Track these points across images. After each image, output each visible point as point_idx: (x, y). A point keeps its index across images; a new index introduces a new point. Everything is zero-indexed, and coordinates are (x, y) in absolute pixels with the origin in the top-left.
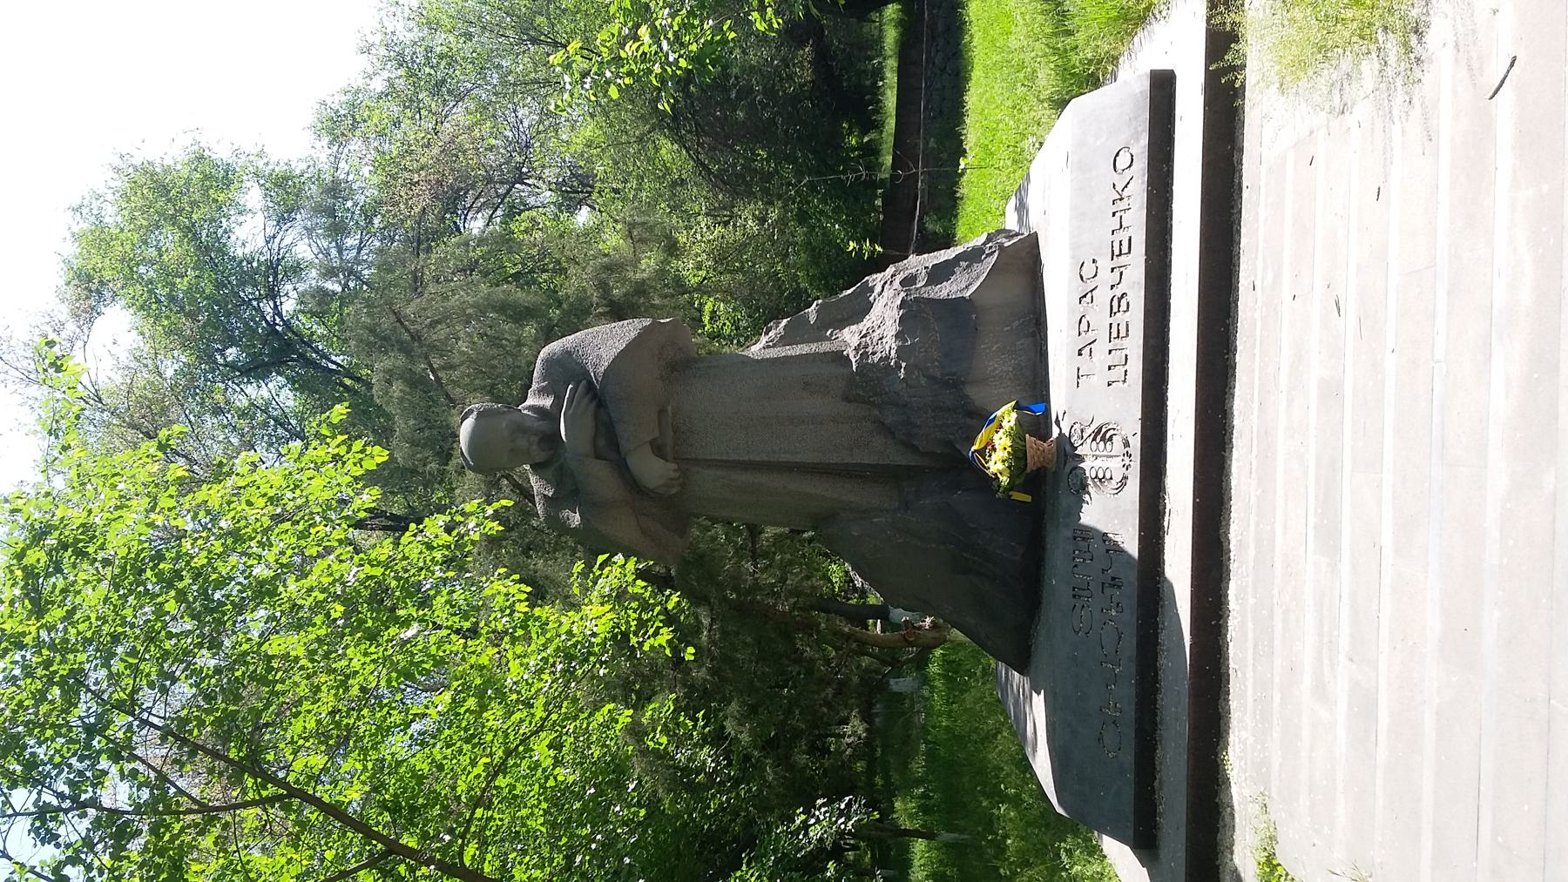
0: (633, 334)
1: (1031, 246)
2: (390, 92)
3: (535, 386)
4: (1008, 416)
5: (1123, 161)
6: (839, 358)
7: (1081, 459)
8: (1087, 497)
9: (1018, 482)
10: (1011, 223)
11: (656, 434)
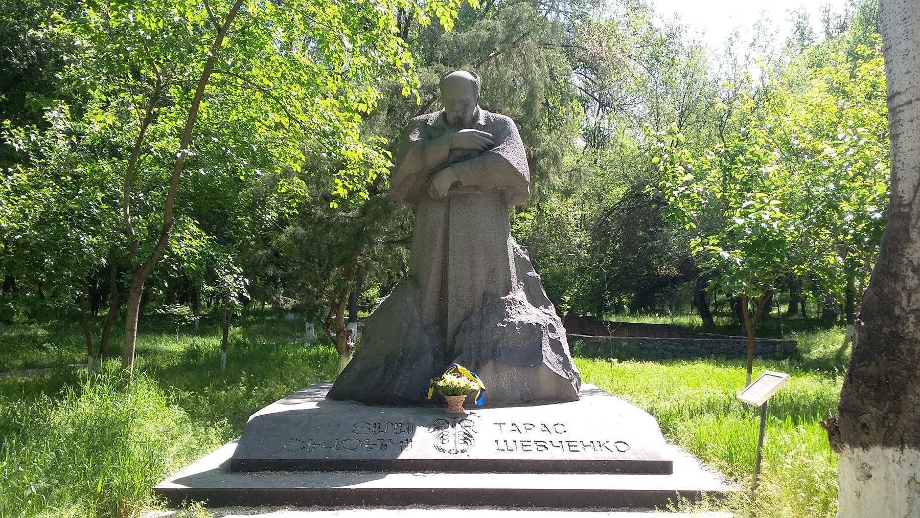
0: (521, 171)
1: (573, 398)
2: (652, 30)
3: (490, 114)
4: (477, 385)
5: (622, 447)
6: (508, 289)
7: (454, 426)
8: (432, 429)
9: (440, 392)
10: (584, 387)
11: (464, 185)
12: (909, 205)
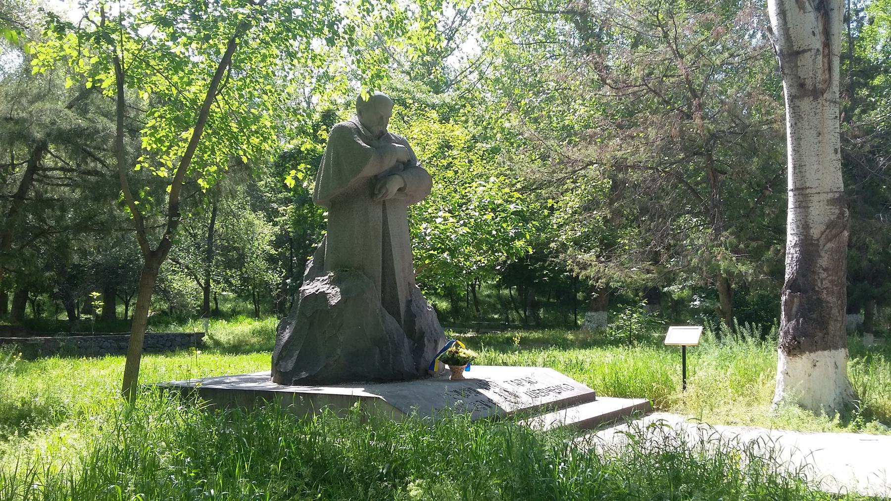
12: (818, 240)
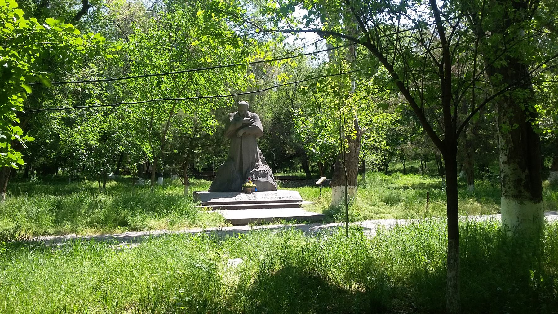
4: (255, 185)
6: (258, 161)
